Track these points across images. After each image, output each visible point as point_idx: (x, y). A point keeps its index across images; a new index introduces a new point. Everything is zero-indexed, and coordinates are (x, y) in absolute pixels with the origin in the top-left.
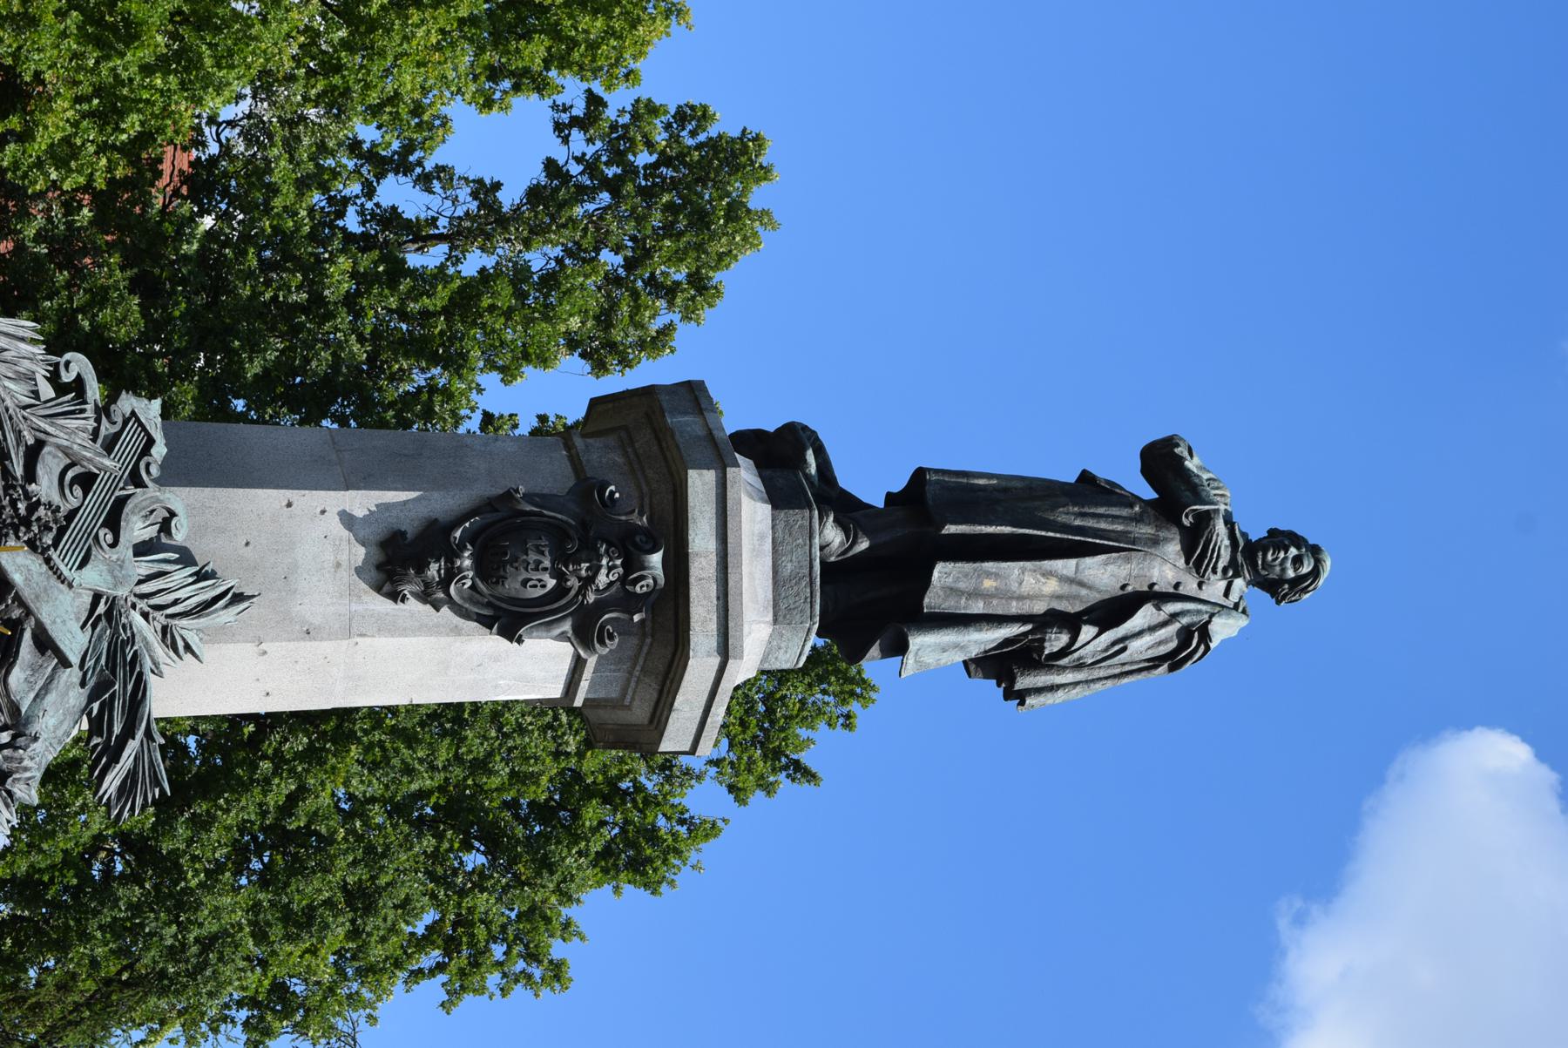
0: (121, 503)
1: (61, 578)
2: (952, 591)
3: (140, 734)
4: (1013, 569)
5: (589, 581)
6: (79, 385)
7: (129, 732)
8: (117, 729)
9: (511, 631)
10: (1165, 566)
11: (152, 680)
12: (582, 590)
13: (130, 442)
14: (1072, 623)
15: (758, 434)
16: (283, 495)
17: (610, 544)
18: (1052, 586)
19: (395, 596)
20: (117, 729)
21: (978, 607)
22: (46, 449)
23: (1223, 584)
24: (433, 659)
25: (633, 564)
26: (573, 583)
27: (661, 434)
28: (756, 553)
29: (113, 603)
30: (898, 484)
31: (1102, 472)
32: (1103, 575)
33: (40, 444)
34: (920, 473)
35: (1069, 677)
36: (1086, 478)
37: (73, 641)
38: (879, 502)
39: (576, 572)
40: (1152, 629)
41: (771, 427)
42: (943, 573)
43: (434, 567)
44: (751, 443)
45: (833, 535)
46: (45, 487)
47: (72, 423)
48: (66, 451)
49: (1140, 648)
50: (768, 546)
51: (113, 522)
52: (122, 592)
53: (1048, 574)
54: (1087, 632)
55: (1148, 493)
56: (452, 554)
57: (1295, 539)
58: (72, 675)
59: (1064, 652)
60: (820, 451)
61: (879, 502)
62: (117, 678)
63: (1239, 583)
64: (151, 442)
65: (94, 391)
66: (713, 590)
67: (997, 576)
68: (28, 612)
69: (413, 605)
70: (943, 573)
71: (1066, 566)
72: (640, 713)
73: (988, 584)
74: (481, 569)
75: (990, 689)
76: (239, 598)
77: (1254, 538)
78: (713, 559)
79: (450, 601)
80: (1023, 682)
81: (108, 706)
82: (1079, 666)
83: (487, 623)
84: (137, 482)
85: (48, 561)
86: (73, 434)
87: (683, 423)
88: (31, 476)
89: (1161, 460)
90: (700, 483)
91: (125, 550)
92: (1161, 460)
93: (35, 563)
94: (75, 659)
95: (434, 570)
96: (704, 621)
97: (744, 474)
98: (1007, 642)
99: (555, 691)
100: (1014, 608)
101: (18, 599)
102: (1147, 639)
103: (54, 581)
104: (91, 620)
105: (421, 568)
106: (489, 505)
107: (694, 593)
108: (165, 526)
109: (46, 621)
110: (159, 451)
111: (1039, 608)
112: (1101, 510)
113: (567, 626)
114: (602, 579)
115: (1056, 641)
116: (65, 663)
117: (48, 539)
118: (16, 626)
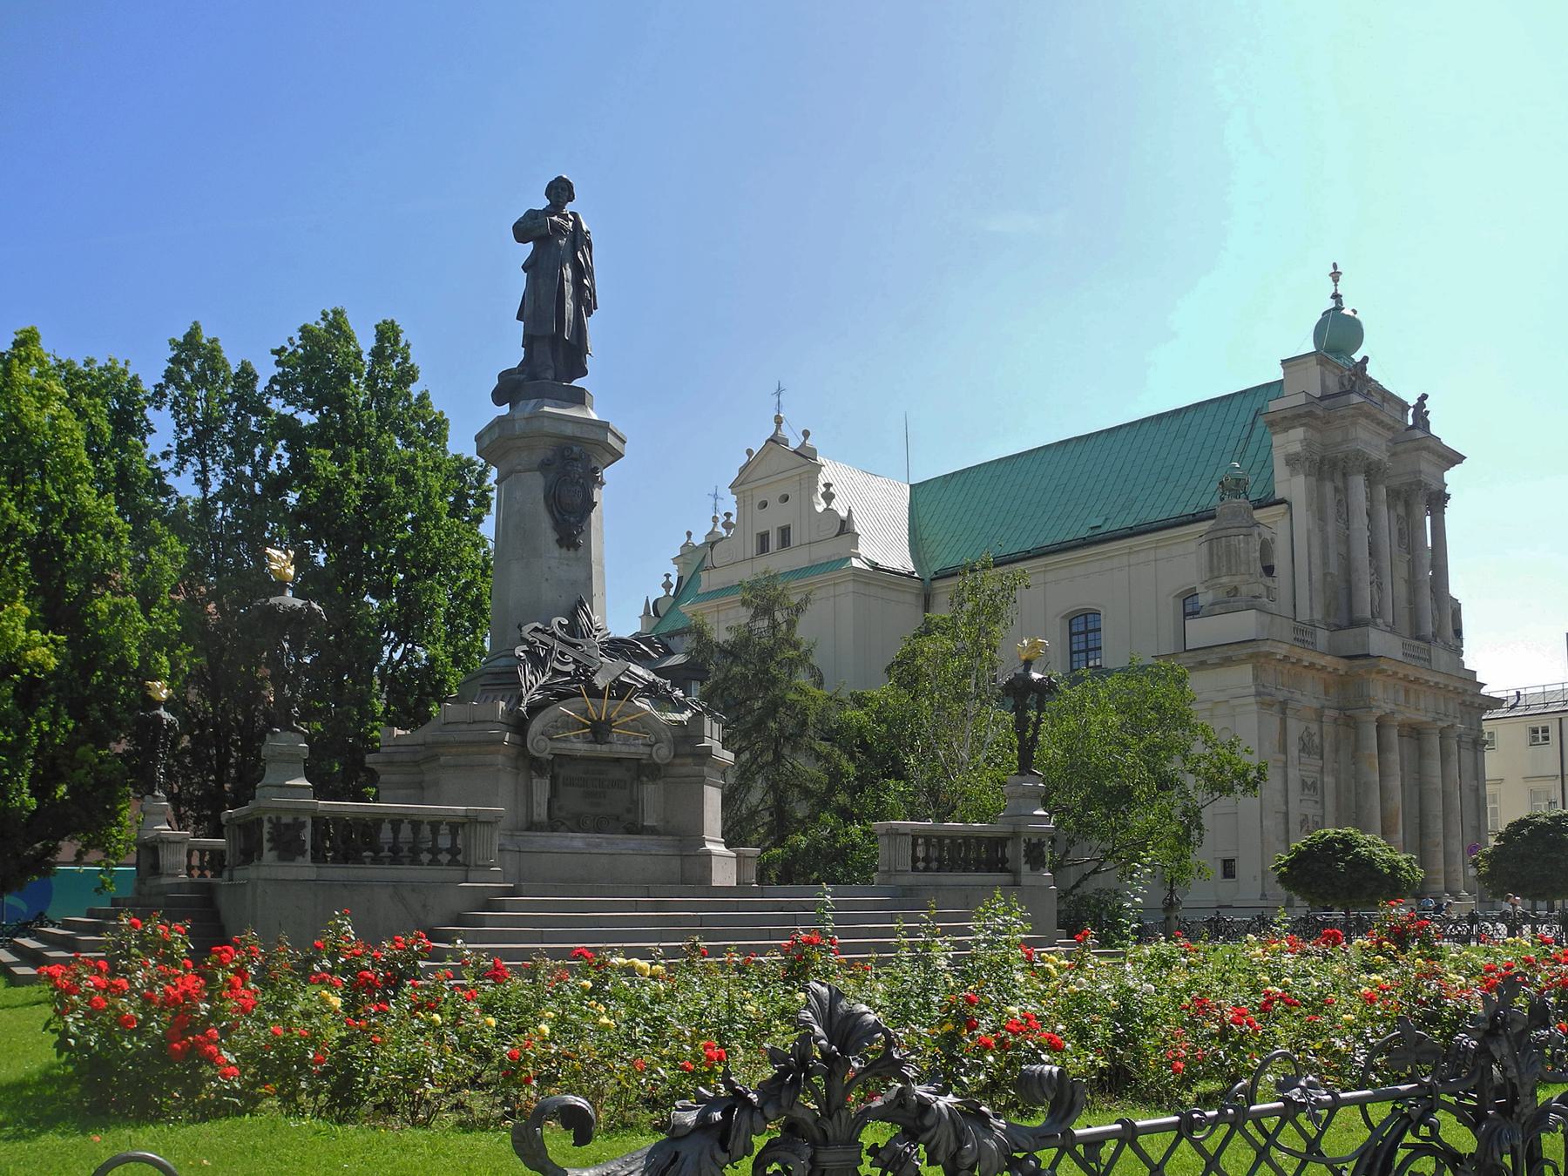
13: (539, 635)
46: (570, 668)
51: (574, 646)
88: (568, 674)
110: (537, 624)
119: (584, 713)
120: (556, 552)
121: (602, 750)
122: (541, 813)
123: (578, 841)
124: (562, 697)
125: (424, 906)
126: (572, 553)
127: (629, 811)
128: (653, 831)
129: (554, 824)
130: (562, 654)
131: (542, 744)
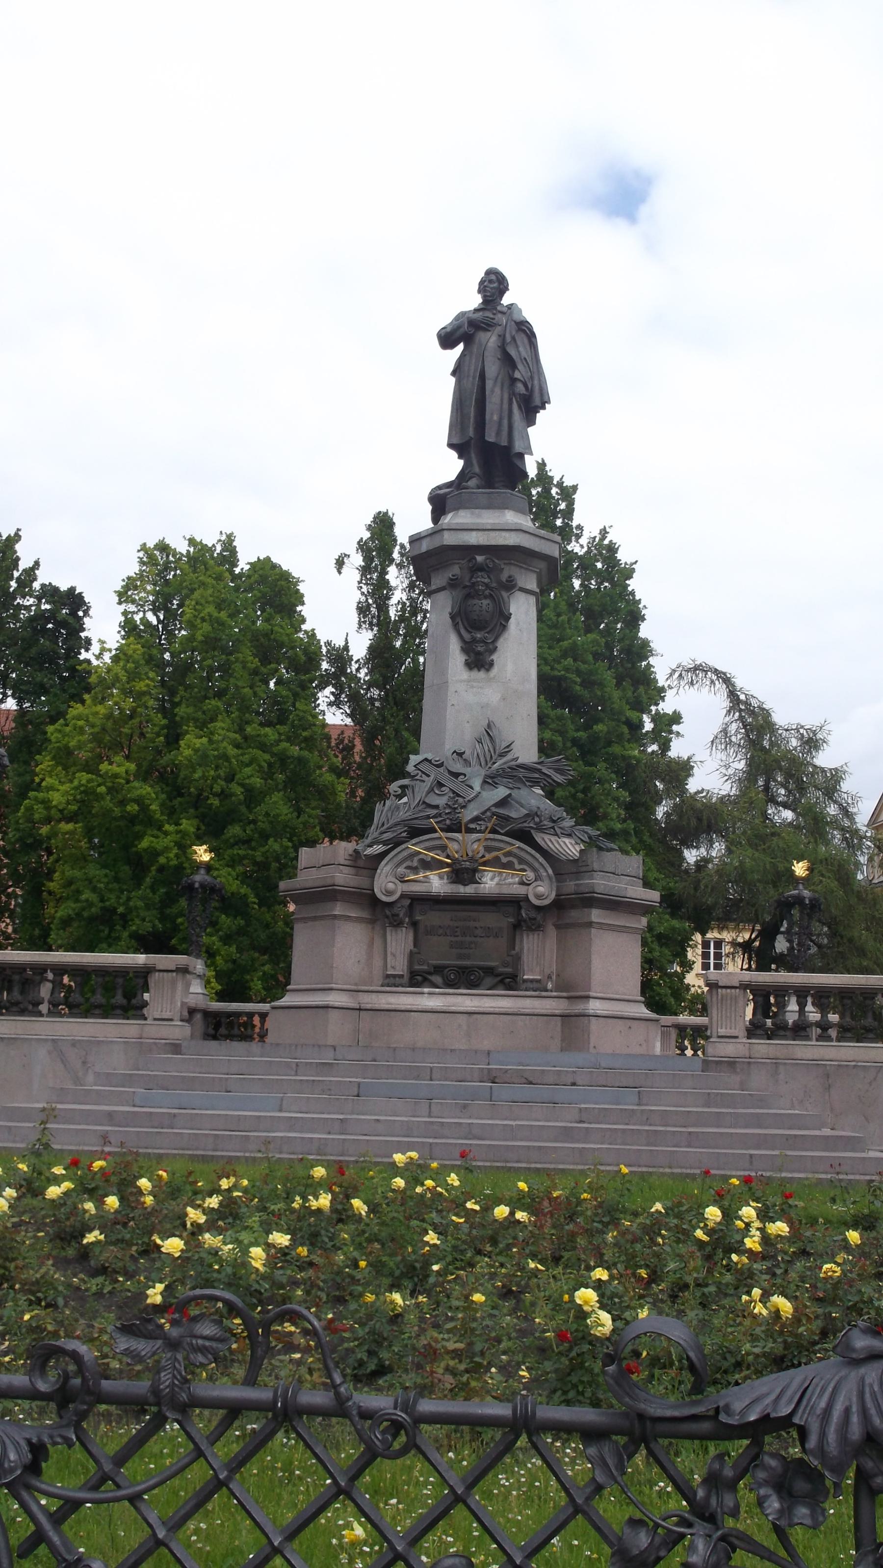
0: (450, 773)
1: (477, 796)
2: (498, 433)
3: (539, 767)
4: (489, 407)
5: (487, 585)
6: (403, 787)
7: (539, 771)
8: (537, 776)
9: (508, 618)
10: (490, 340)
11: (520, 761)
12: (491, 589)
13: (425, 767)
14: (513, 380)
15: (433, 512)
16: (449, 709)
17: (472, 577)
18: (498, 390)
19: (492, 664)
20: (537, 776)
21: (505, 422)
22: (427, 801)
23: (500, 315)
24: (519, 649)
25: (481, 568)
26: (487, 592)
27: (429, 554)
28: (479, 516)
29: (487, 776)
30: (454, 454)
31: (451, 368)
32: (493, 369)
33: (424, 802)
34: (451, 445)
35: (536, 382)
36: (454, 373)
37: (501, 792)
38: (461, 463)
39: (483, 591)
40: (517, 347)
41: (430, 507)
42: (490, 437)
43: (479, 649)
44: (437, 515)
45: (473, 482)
46: (441, 801)
47: (416, 790)
48: (428, 793)
49: (524, 351)
50: (477, 511)
51: (456, 775)
52: (483, 772)
53: (492, 391)
54: (517, 375)
55: (460, 347)
56: (474, 640)
57: (482, 282)
58: (515, 793)
59: (525, 385)
60: (439, 488)
61: (461, 463)
62: (520, 775)
63: (499, 308)
64: (426, 760)
65: (405, 782)
66: (493, 534)
67: (492, 414)
68: (489, 809)
69: (494, 657)
70: (490, 437)
71: (489, 384)
72: (542, 565)
73: (495, 418)
74: (479, 629)
75: (541, 416)
76: (489, 726)
77: (481, 301)
78: (480, 533)
79: (493, 642)
80: (537, 401)
81: (529, 779)
82: (532, 378)
83: (504, 627)
84: (441, 765)
85: (469, 801)
86: (421, 789)
87: (425, 546)
88: (437, 807)
89: (447, 339)
90: (450, 539)
91: (467, 770)
92: (447, 339)
93: (471, 806)
94: (508, 792)
95: (480, 648)
96: (505, 538)
97: (447, 519)
98: (520, 407)
99: (532, 600)
100: (506, 406)
101: (484, 813)
102: (521, 349)
103: (478, 799)
104: (495, 785)
105: (479, 653)
106: (455, 626)
107: (493, 543)
108: (460, 754)
109: (493, 802)
110: (429, 756)
111: (506, 396)
112: (466, 369)
113: (505, 594)
114: (487, 581)
115: (520, 388)
116: (510, 795)
117: (461, 800)
118: (494, 814)
119: (443, 848)
120: (465, 674)
121: (469, 890)
122: (399, 965)
123: (431, 1000)
124: (415, 832)
125: (84, 1063)
126: (482, 674)
127: (506, 965)
128: (538, 987)
129: (417, 978)
130: (440, 785)
131: (391, 886)
